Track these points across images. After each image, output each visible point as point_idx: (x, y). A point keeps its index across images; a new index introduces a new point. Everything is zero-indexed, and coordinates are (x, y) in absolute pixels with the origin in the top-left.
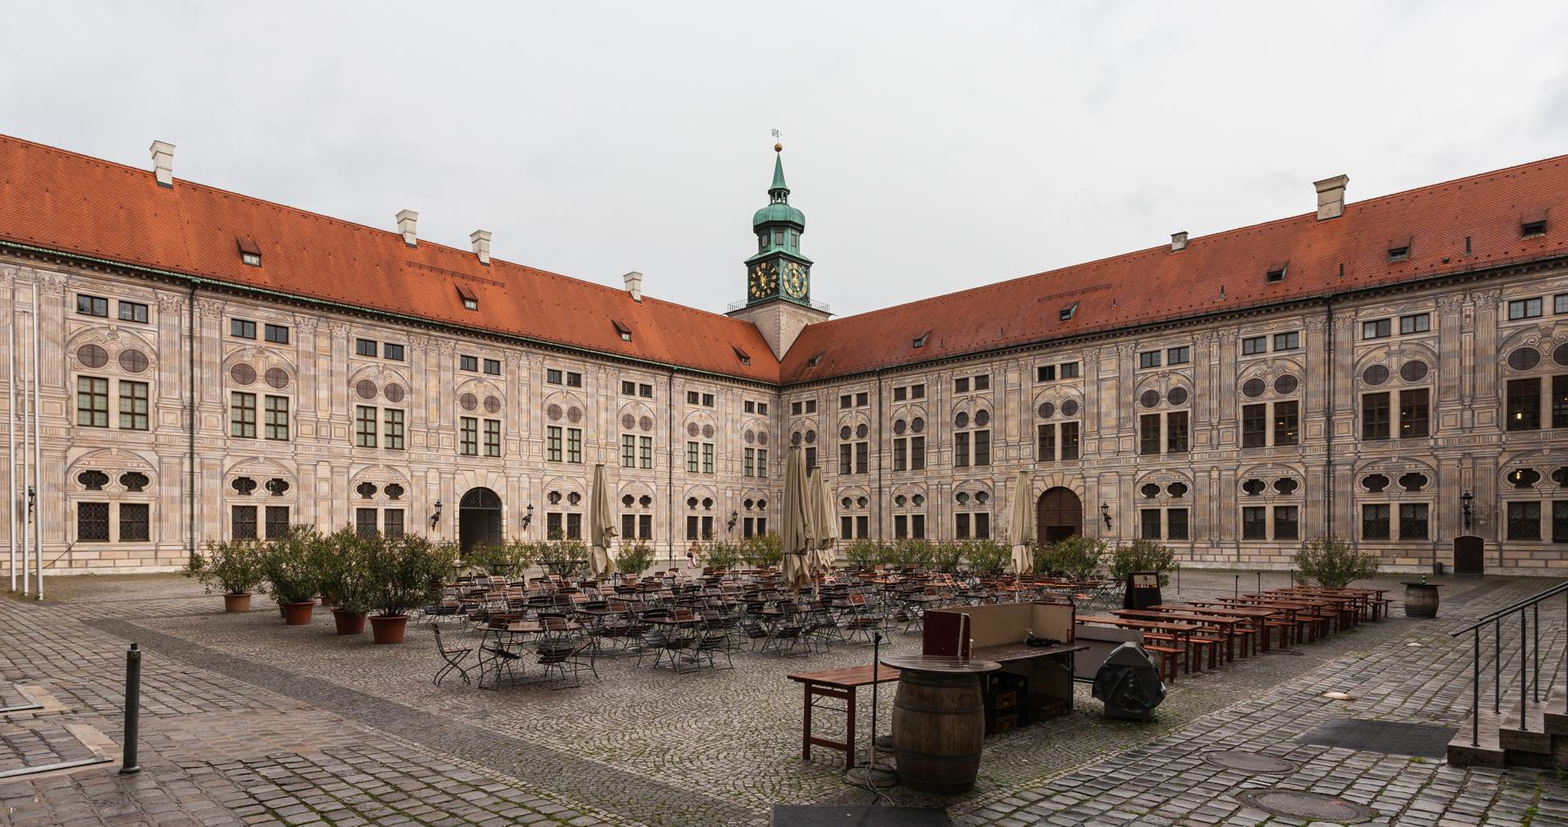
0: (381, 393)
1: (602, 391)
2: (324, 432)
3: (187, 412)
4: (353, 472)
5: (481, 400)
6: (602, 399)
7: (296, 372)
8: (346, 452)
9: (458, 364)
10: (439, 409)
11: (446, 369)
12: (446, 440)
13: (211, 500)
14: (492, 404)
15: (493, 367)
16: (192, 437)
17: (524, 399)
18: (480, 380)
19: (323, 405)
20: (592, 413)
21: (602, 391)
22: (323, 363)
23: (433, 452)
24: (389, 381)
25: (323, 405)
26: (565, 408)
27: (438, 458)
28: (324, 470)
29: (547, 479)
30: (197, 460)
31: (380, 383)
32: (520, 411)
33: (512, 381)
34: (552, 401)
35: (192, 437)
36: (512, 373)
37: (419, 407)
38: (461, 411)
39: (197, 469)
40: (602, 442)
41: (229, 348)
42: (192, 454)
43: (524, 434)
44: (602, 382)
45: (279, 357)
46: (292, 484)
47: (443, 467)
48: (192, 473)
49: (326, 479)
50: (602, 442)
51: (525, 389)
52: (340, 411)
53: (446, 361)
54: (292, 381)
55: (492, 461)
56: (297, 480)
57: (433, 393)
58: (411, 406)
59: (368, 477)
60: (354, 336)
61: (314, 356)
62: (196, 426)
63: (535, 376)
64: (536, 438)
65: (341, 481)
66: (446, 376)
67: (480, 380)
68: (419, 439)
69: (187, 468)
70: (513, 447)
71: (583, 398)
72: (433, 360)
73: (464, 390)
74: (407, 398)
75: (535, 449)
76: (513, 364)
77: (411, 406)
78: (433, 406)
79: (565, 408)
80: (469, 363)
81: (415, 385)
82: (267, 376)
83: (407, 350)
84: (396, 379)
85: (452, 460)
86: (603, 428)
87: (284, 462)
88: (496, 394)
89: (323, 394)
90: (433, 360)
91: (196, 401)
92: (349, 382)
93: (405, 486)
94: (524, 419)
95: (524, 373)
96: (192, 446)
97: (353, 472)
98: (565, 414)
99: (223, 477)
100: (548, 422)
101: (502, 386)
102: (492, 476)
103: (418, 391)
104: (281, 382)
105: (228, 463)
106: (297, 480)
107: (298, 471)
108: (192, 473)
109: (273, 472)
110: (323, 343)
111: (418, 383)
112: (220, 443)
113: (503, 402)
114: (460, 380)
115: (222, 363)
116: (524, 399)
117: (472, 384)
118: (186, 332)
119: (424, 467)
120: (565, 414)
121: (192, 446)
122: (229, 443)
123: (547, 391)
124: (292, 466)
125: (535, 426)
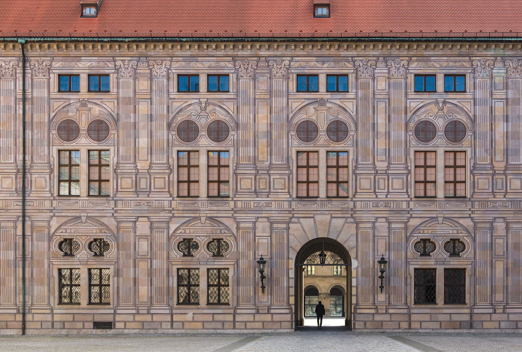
0: (203, 133)
1: (500, 94)
2: (143, 184)
3: (20, 175)
4: (173, 227)
5: (323, 126)
6: (499, 106)
7: (117, 121)
8: (166, 204)
9: (293, 85)
10: (270, 145)
11: (279, 94)
12: (278, 181)
13: (40, 264)
14: (338, 130)
15: (337, 84)
16: (24, 200)
17: (381, 120)
18: (322, 102)
19: (143, 154)
20: (483, 127)
21: (500, 94)
22: (143, 108)
23: (263, 199)
24: (212, 118)
25: (143, 154)
26: (440, 124)
27: (268, 204)
28: (143, 227)
29: (414, 222)
30: (28, 223)
31: (202, 122)
32: (376, 135)
33: (365, 98)
34: (422, 116)
35: (24, 200)
36: (365, 87)
37: (246, 144)
38: (296, 145)
39: (28, 233)
40: (500, 166)
41: (56, 105)
42: (24, 216)
43: (381, 165)
44: (498, 80)
45: (102, 107)
46: (113, 244)
47: (275, 216)
48: (24, 236)
49: (145, 237)
50: (500, 166)
51: (382, 106)
52: (160, 159)
53: (279, 85)
54: (113, 132)
55: (336, 204)
56: (117, 239)
57: (262, 126)
58: (237, 145)
59: (189, 232)
60: (174, 72)
61: (133, 101)
62: (28, 189)
63: (397, 86)
64: (398, 168)
65: (161, 238)
66: (279, 102)
67: (322, 102)
68: (246, 184)
69: (19, 232)
70: (365, 183)
71: (468, 107)
72: (263, 86)
73: (302, 117)
74: (233, 135)
75: (397, 184)
76: (365, 77)
77: (237, 145)
78: (263, 142)
79: (440, 124)
80: (306, 83)
81: (242, 119)
82: (89, 130)
83: (232, 78)
84: (221, 115)
85: (286, 205)
86: (500, 146)
87: (105, 220)
88: (342, 117)
89: (143, 142)
90: (263, 86)
91: (28, 163)
92: (169, 125)
93: (231, 241)
94: (381, 145)
95: (382, 85)
96: (24, 209)
97: (173, 227)
98: (440, 133)
99: (50, 238)
100: (415, 145)
101: (350, 106)
102: (338, 223)
103: (246, 126)
104: (102, 134)
105: (55, 224)
106: (117, 239)
107: (118, 228)
108: (24, 236)
109: (95, 231)
110: (143, 85)
111: (245, 116)
112: (47, 204)
113: (352, 127)
114: (295, 105)
115: (50, 121)
116: (381, 120)
117: (311, 109)
118: (20, 96)
119: (252, 217)
120: (440, 133)
121: (24, 209)
122: (55, 203)
123: (413, 105)
124: (111, 223)
125: (397, 152)
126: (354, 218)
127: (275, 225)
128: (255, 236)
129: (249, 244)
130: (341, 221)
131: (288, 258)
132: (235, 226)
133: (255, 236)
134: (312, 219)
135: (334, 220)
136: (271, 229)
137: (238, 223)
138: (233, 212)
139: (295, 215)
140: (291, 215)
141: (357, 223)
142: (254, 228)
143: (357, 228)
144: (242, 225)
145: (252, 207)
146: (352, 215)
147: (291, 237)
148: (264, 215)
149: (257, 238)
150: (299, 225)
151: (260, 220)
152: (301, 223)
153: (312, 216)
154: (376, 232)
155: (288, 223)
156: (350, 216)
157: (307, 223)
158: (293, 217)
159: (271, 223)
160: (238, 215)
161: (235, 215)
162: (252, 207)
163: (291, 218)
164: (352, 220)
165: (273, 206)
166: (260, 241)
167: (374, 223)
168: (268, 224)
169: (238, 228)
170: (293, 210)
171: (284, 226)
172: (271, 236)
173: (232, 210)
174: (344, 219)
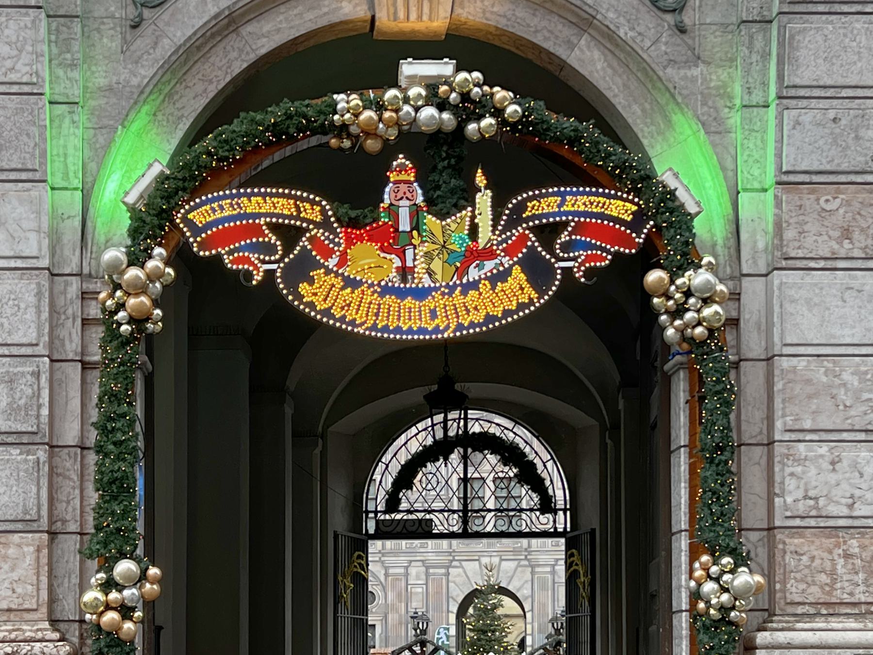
126: (528, 560)
127: (431, 571)
128: (407, 584)
129: (399, 595)
130: (513, 565)
131: (448, 611)
132: (383, 572)
133: (407, 584)
134: (477, 563)
135: (504, 563)
136: (427, 574)
137: (386, 569)
138: (380, 555)
139: (456, 558)
140: (451, 558)
141: (533, 567)
142: (407, 575)
143: (533, 573)
144: (391, 571)
145: (404, 548)
146: (526, 556)
147: (451, 585)
148: (418, 558)
149: (409, 587)
150: (460, 570)
151: (413, 564)
152: (463, 568)
153: (477, 558)
154: (556, 577)
155: (448, 567)
156: (523, 557)
157: (472, 567)
158: (454, 560)
159: (427, 568)
160: (386, 558)
161: (383, 559)
162: (404, 548)
163: (452, 561)
164: (526, 563)
165: (430, 547)
166: (413, 590)
167: (553, 566)
168: (424, 569)
169: (386, 575)
170: (454, 551)
171: (443, 571)
172: (426, 584)
173: (380, 552)
174: (516, 563)
